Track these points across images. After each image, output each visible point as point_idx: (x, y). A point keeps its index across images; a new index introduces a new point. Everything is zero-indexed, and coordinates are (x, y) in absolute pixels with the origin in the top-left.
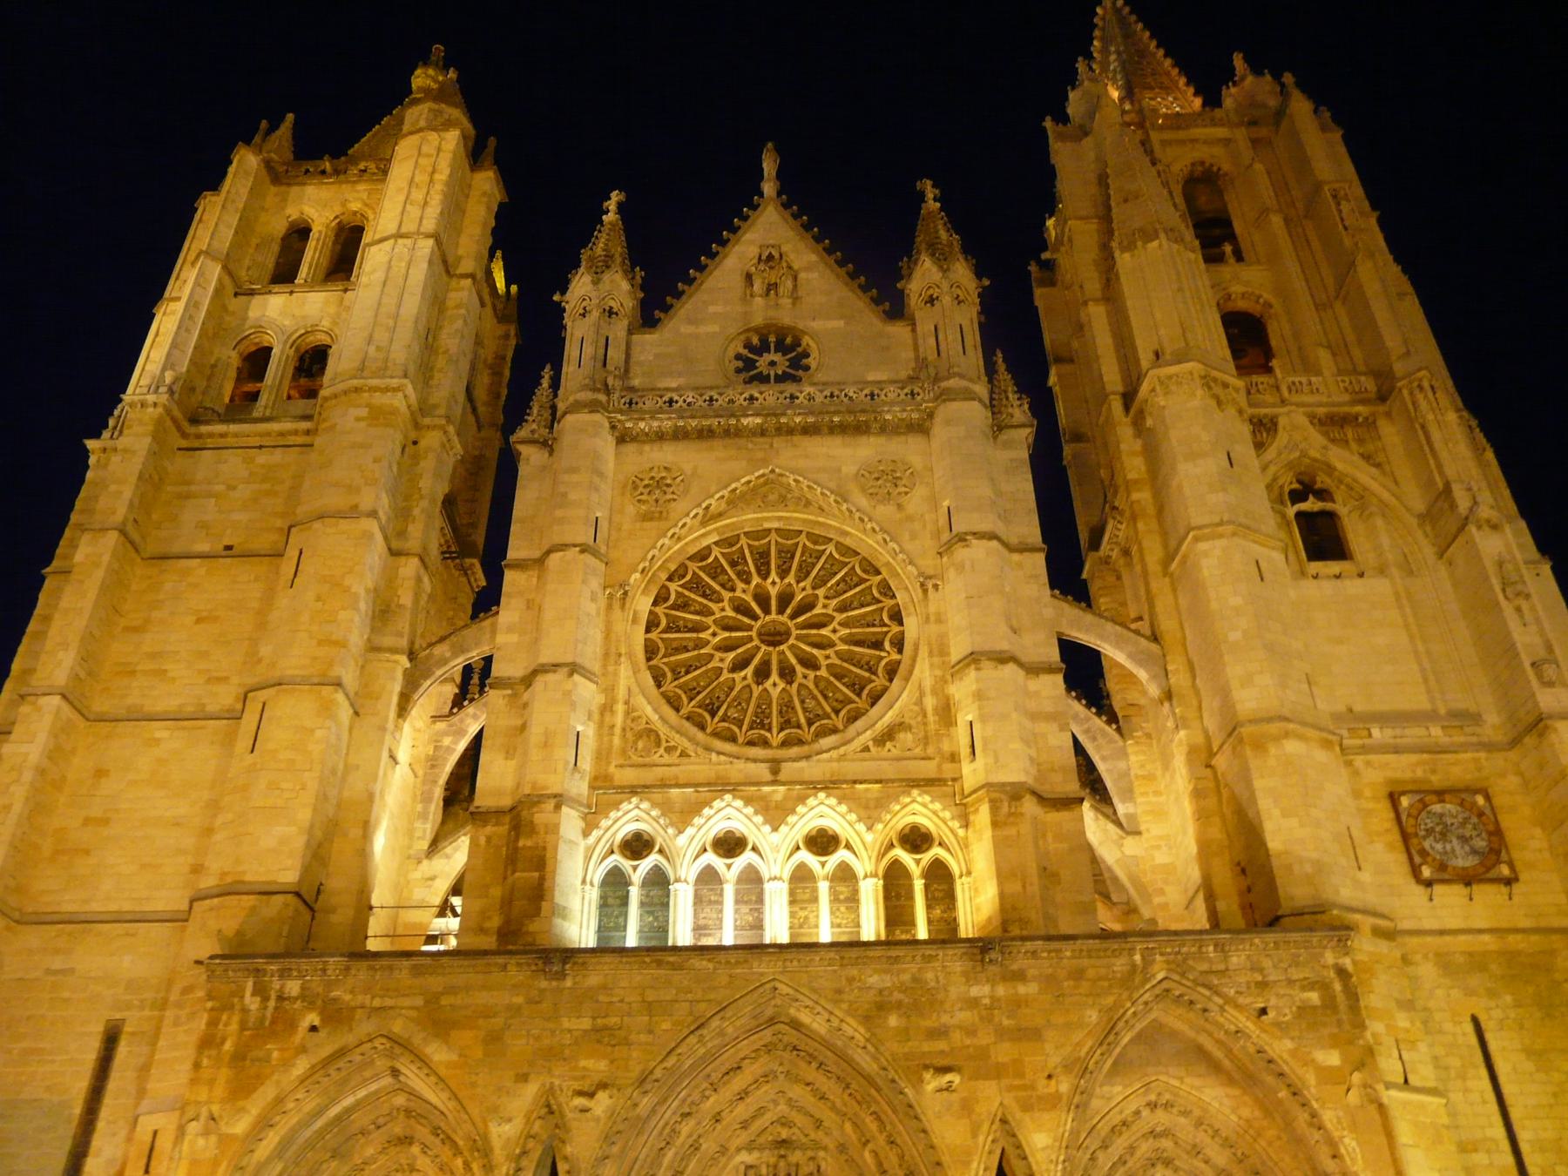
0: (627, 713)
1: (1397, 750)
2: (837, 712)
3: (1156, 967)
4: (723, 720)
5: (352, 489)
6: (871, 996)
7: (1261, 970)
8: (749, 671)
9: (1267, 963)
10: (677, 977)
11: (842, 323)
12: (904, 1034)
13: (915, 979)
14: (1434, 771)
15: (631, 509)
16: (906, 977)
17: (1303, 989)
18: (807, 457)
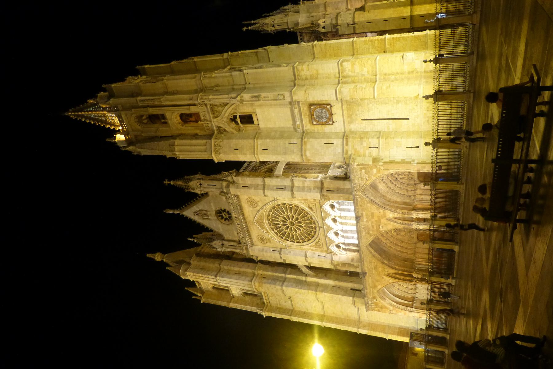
0: (312, 247)
1: (302, 120)
2: (307, 216)
3: (359, 194)
4: (311, 233)
5: (277, 290)
6: (367, 235)
7: (358, 178)
8: (301, 228)
9: (357, 177)
10: (365, 259)
11: (212, 204)
12: (373, 231)
13: (364, 228)
14: (306, 114)
15: (268, 244)
16: (363, 230)
17: (362, 172)
18: (250, 216)
